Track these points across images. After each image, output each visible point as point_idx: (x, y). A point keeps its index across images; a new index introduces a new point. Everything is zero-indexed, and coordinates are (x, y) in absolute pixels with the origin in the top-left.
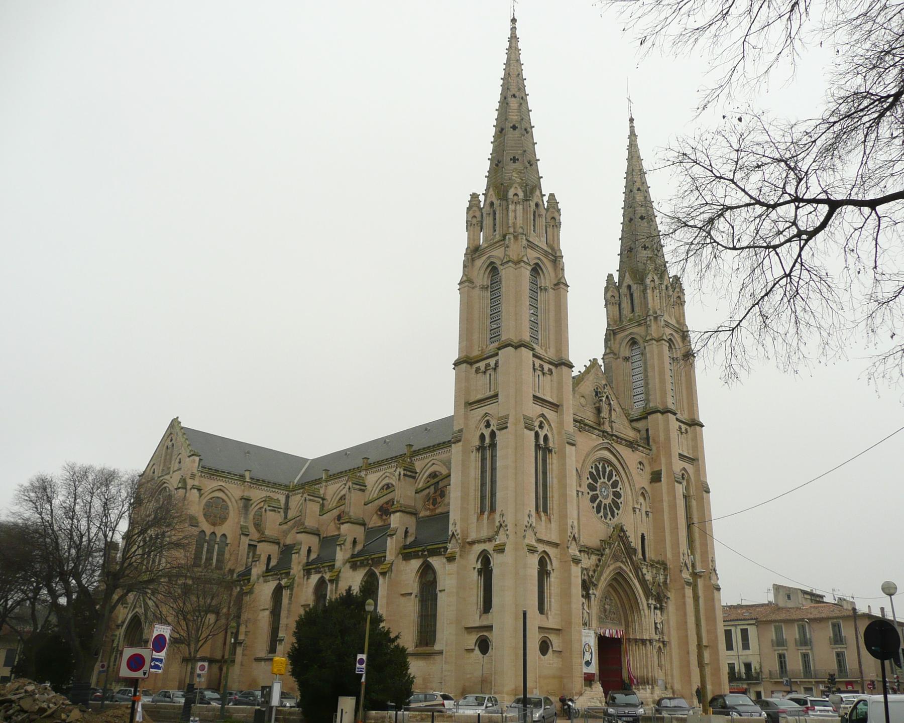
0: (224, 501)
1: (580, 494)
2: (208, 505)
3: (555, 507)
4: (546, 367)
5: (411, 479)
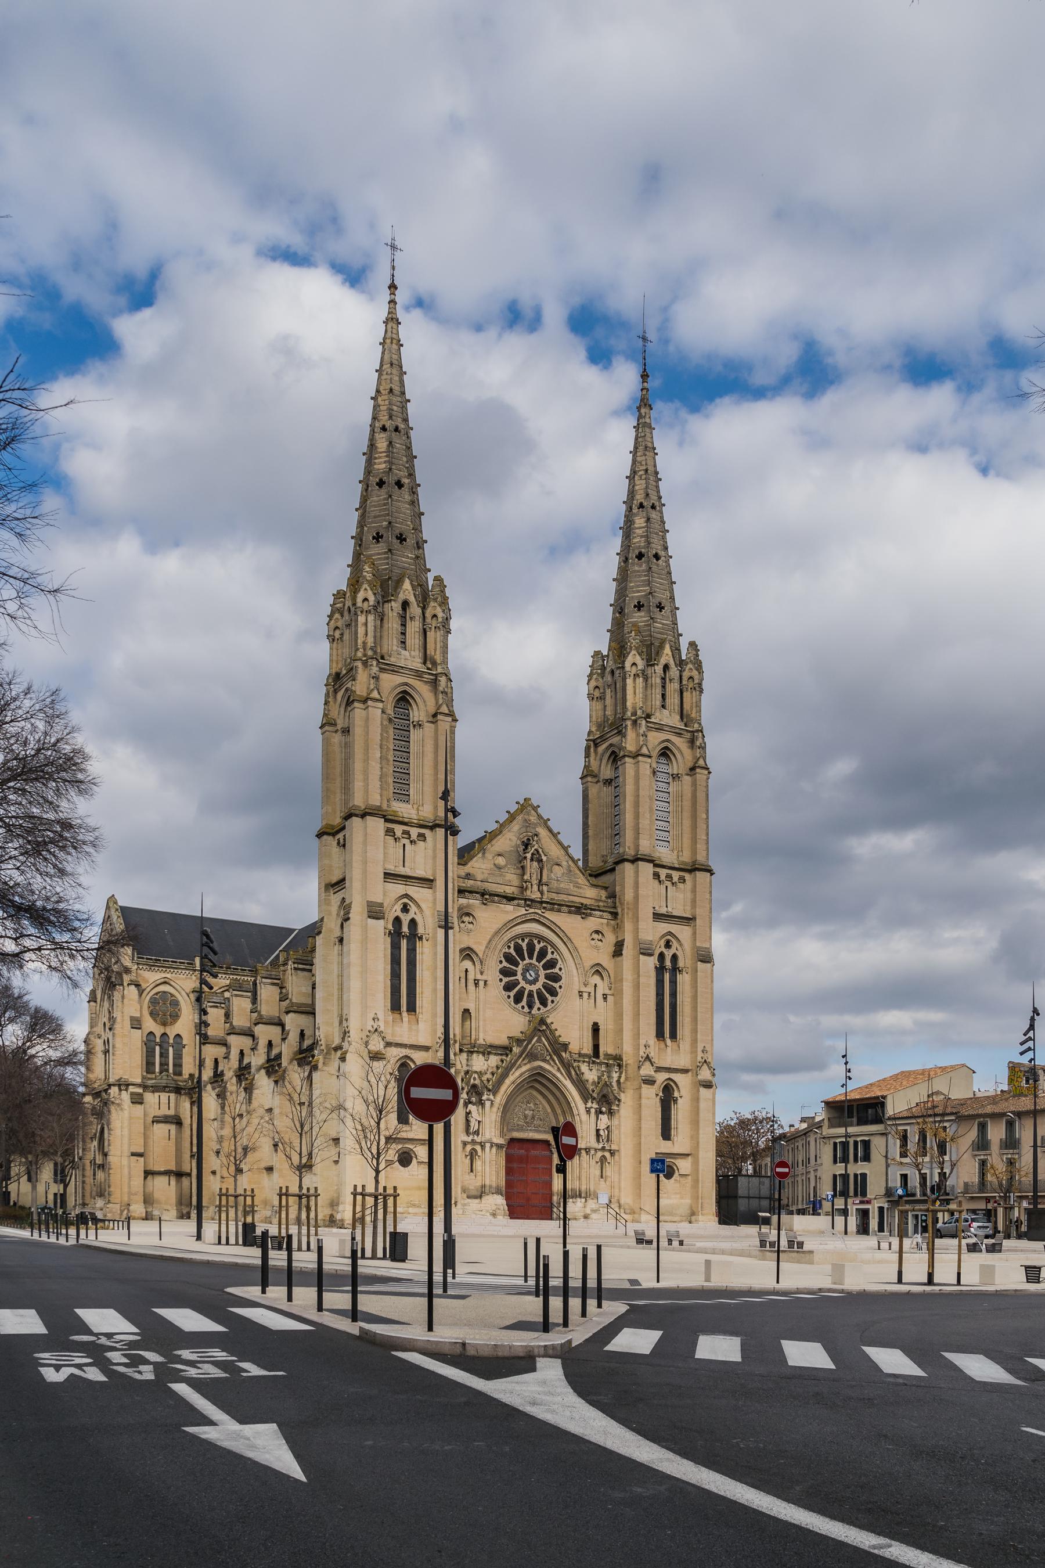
0: (172, 995)
1: (481, 983)
2: (153, 1002)
3: (425, 1005)
4: (414, 832)
5: (306, 973)
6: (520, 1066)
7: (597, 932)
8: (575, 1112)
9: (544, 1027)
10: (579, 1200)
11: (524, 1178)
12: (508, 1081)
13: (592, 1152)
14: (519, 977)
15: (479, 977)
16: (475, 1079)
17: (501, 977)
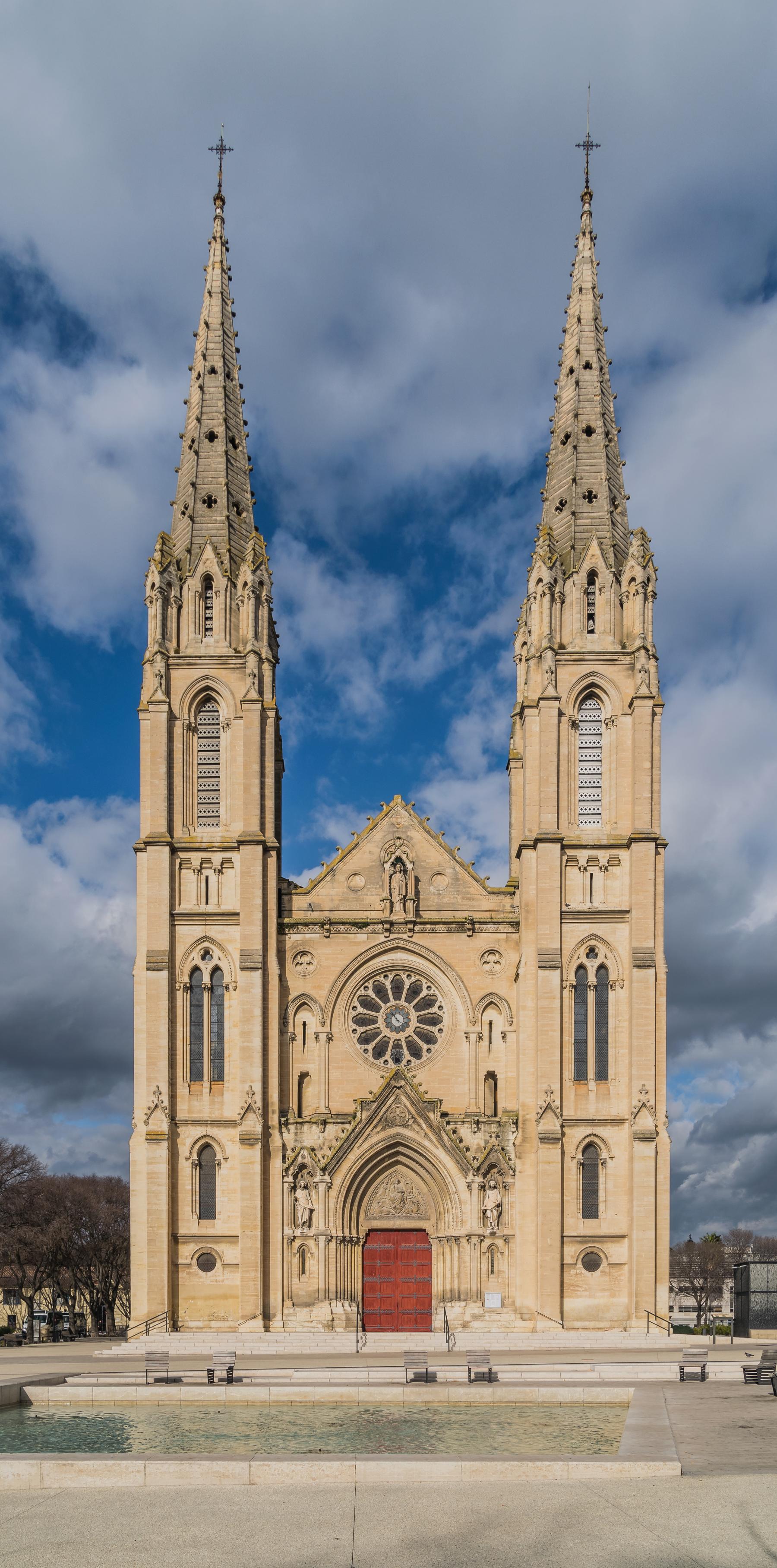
7: (492, 952)
8: (452, 1189)
9: (402, 1083)
10: (457, 1304)
12: (352, 1157)
13: (475, 1240)
14: (381, 1024)
15: (320, 1029)
17: (355, 1026)
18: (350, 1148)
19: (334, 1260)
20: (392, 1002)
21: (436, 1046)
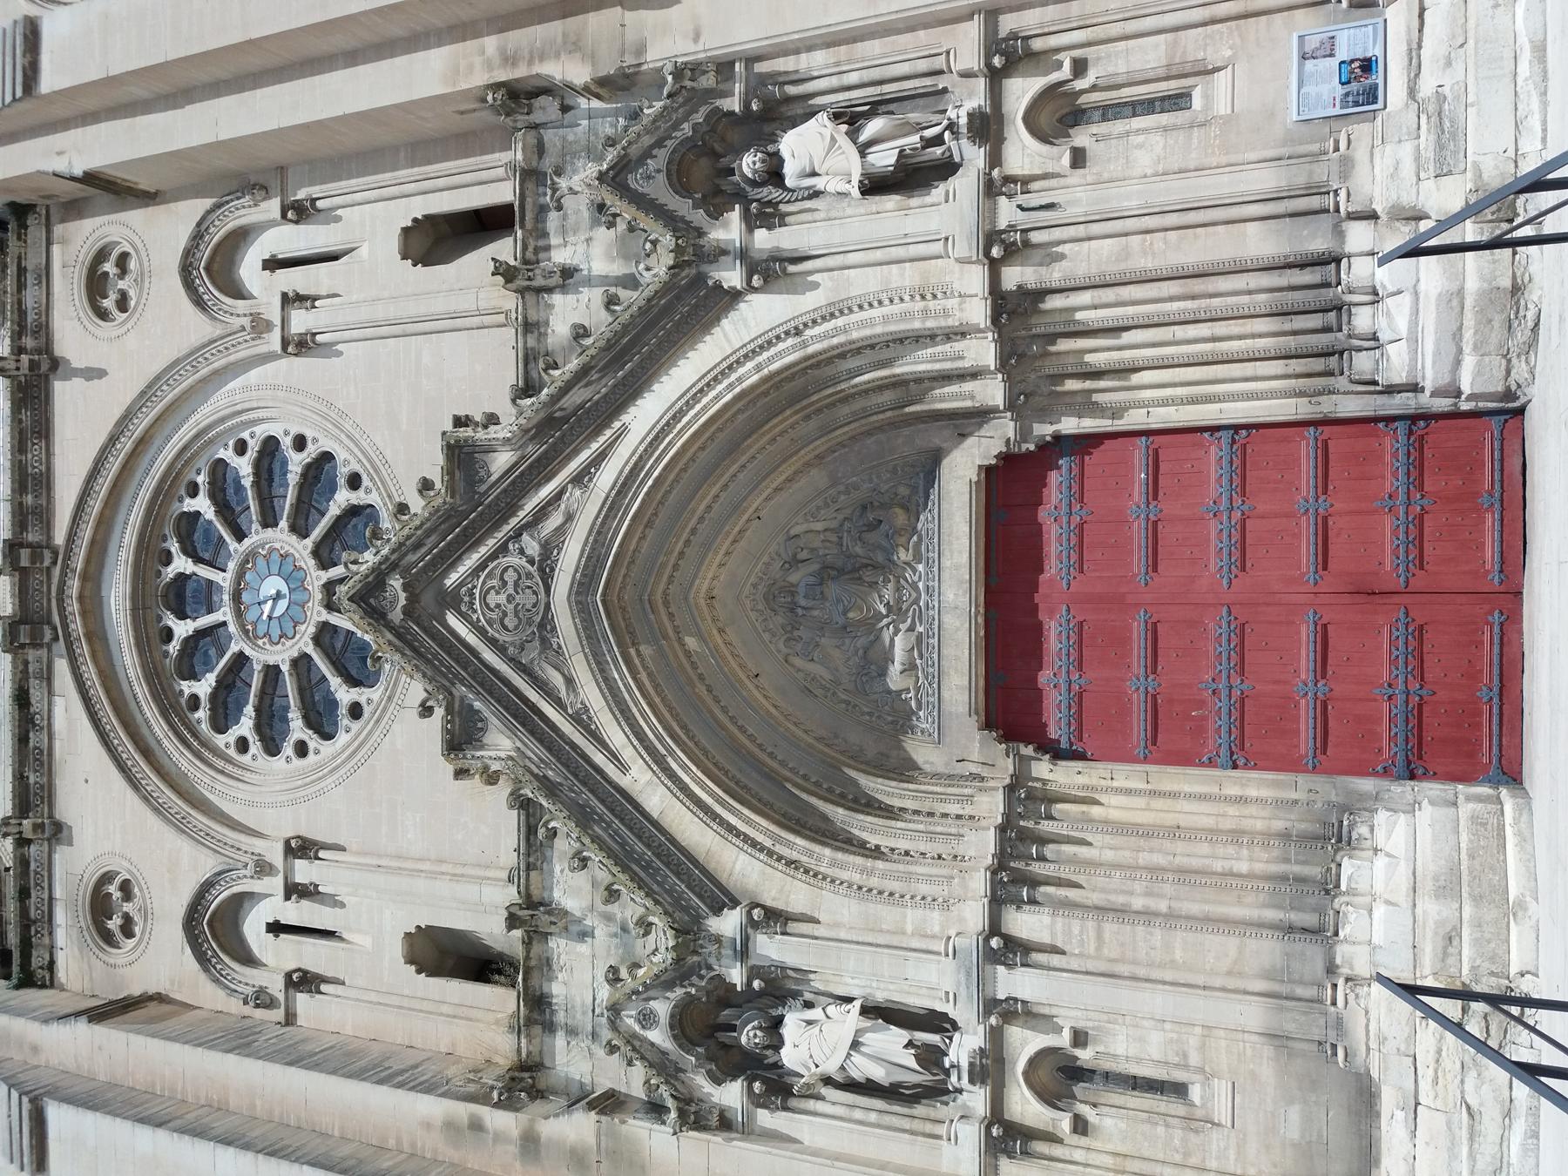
6: (581, 719)
8: (785, 355)
9: (396, 583)
11: (1218, 626)
12: (656, 798)
13: (1007, 212)
16: (647, 1019)
18: (625, 806)
19: (1109, 928)
20: (224, 614)
21: (341, 455)
